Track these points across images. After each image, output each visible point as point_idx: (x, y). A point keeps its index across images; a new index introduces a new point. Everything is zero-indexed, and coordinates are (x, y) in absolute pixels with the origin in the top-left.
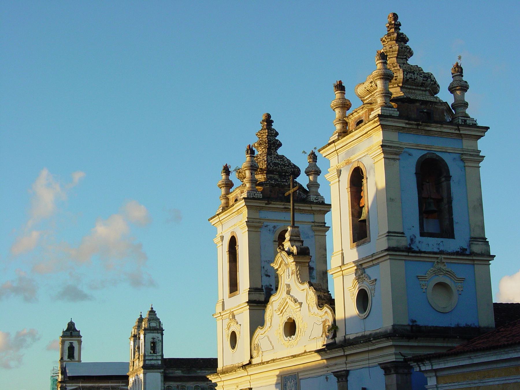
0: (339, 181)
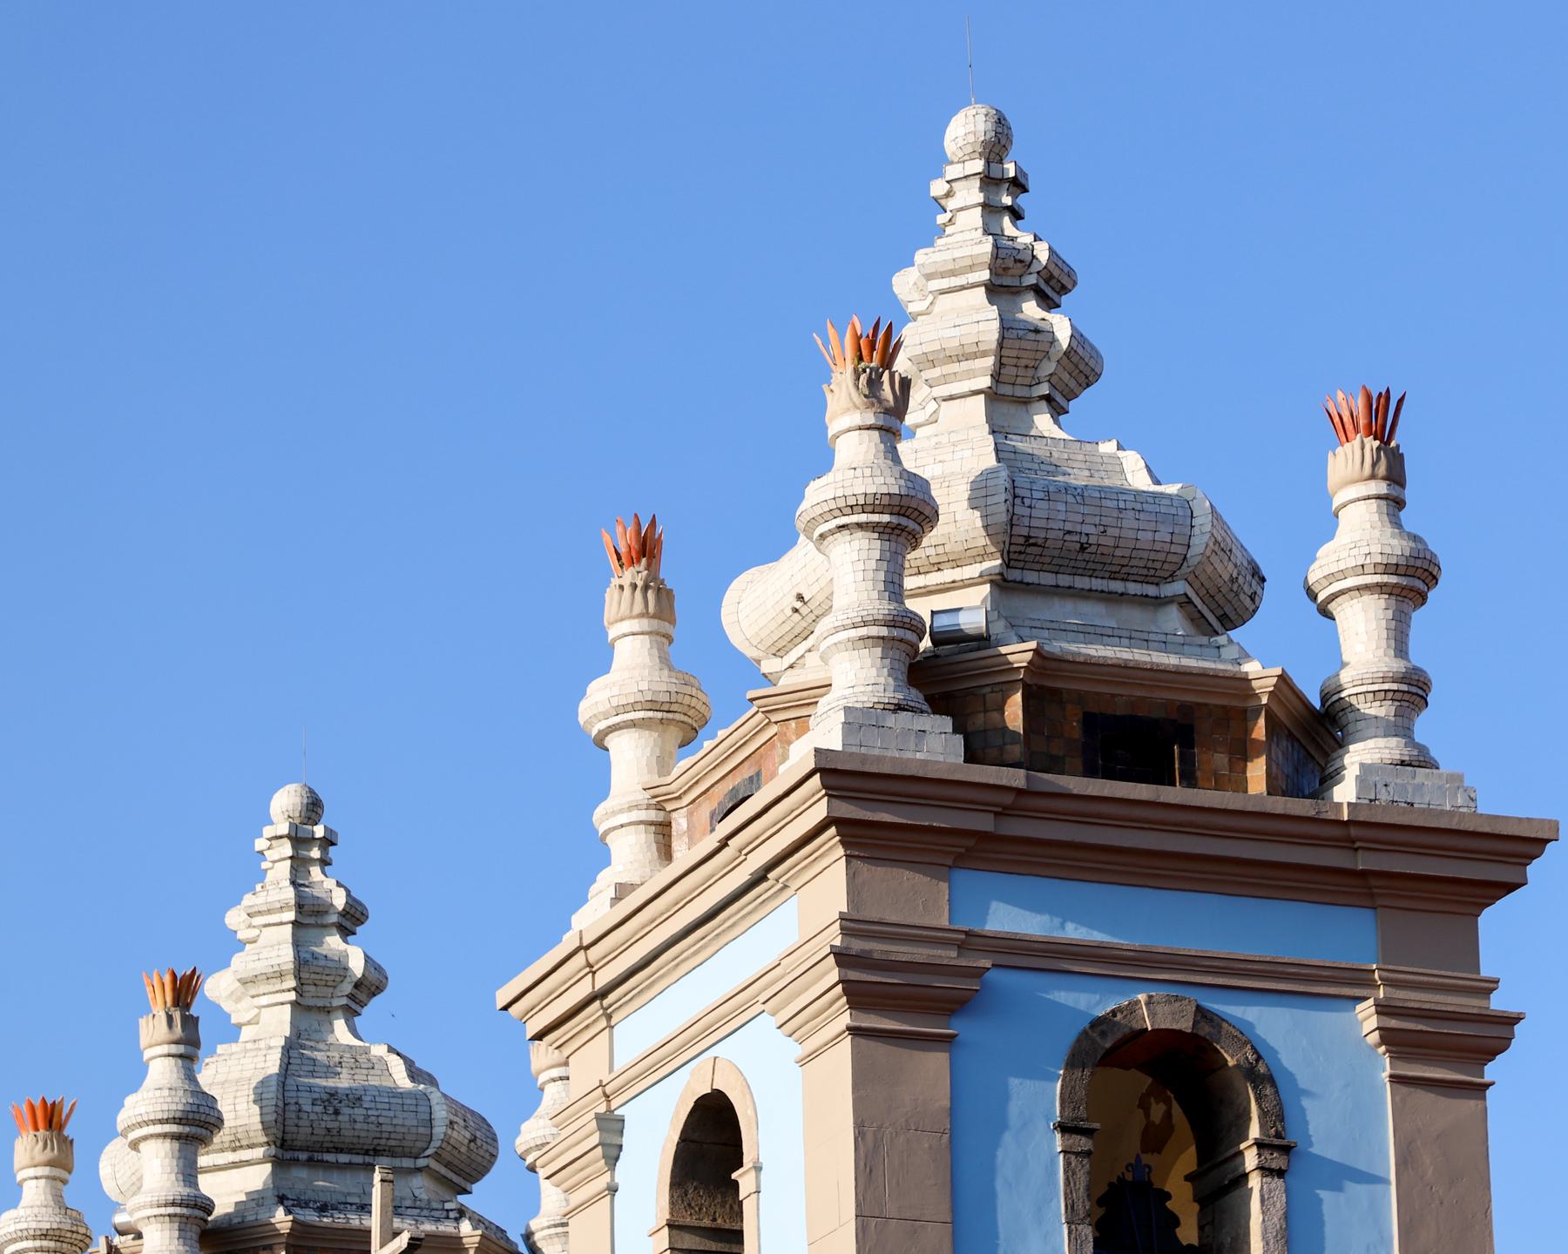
0: (613, 1190)
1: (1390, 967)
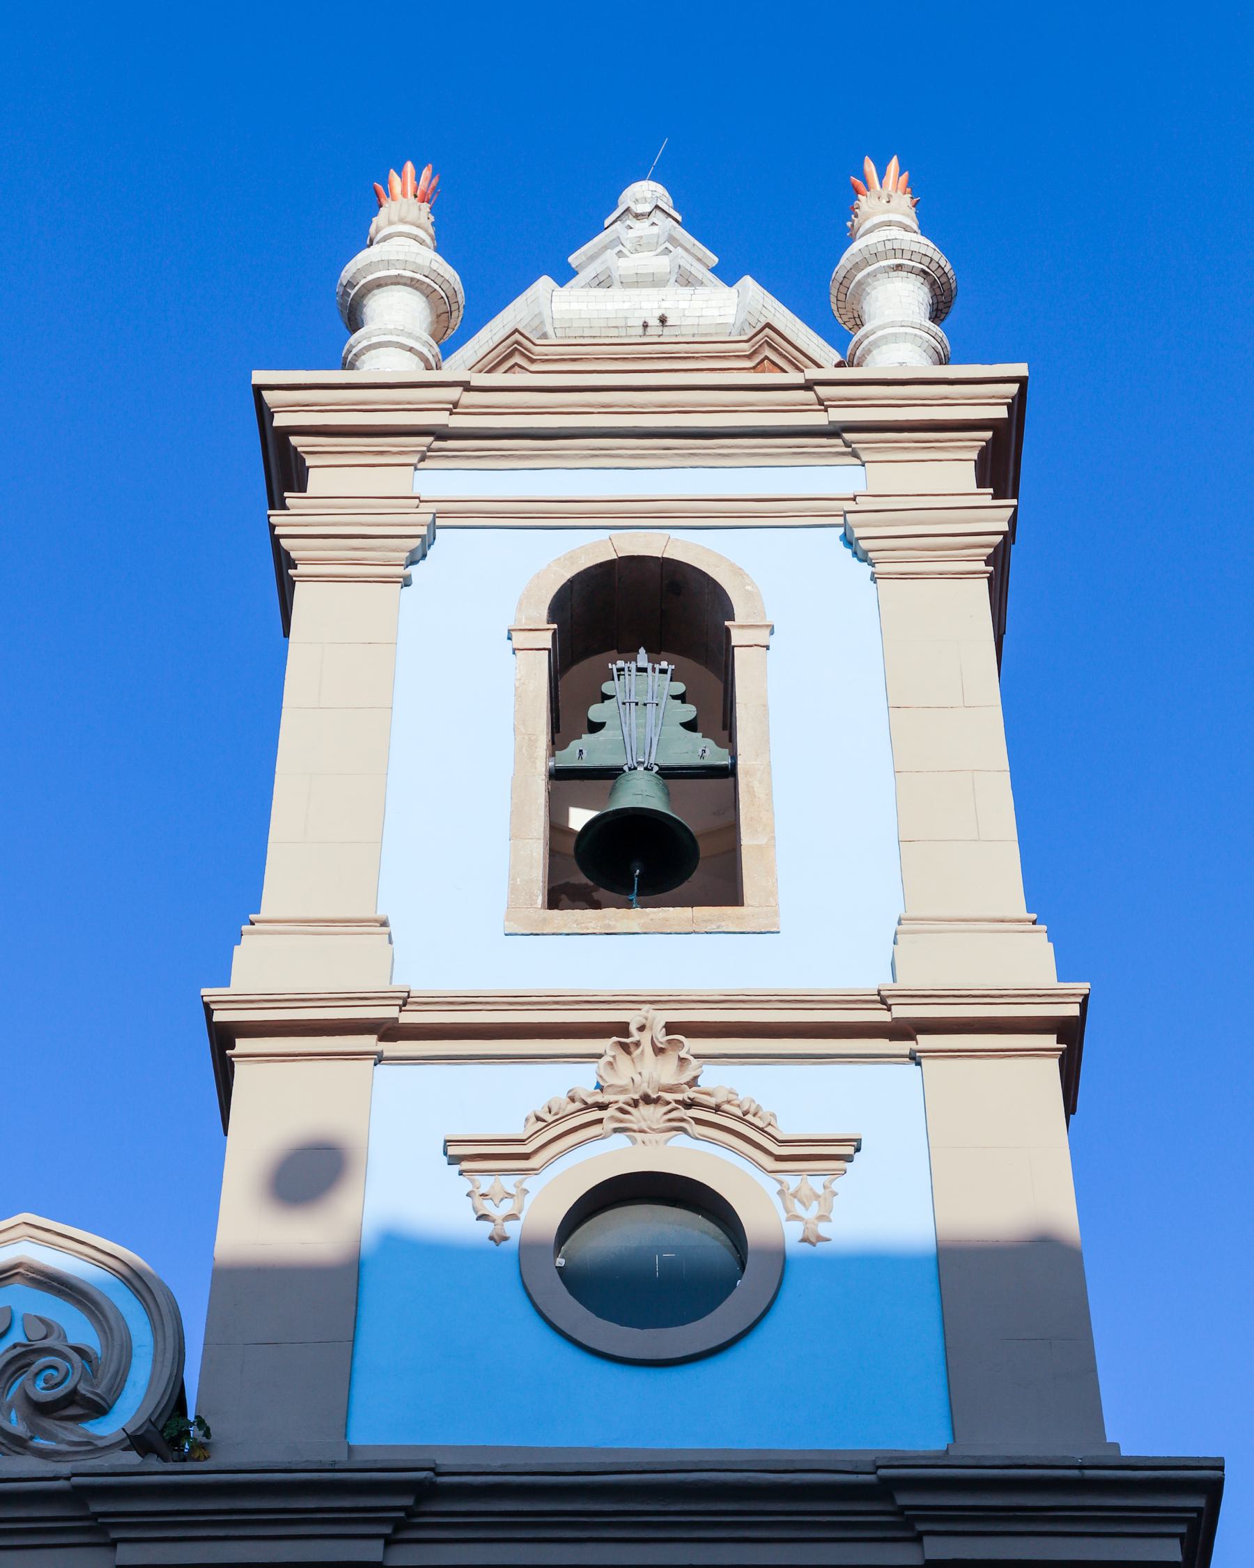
0: (407, 582)
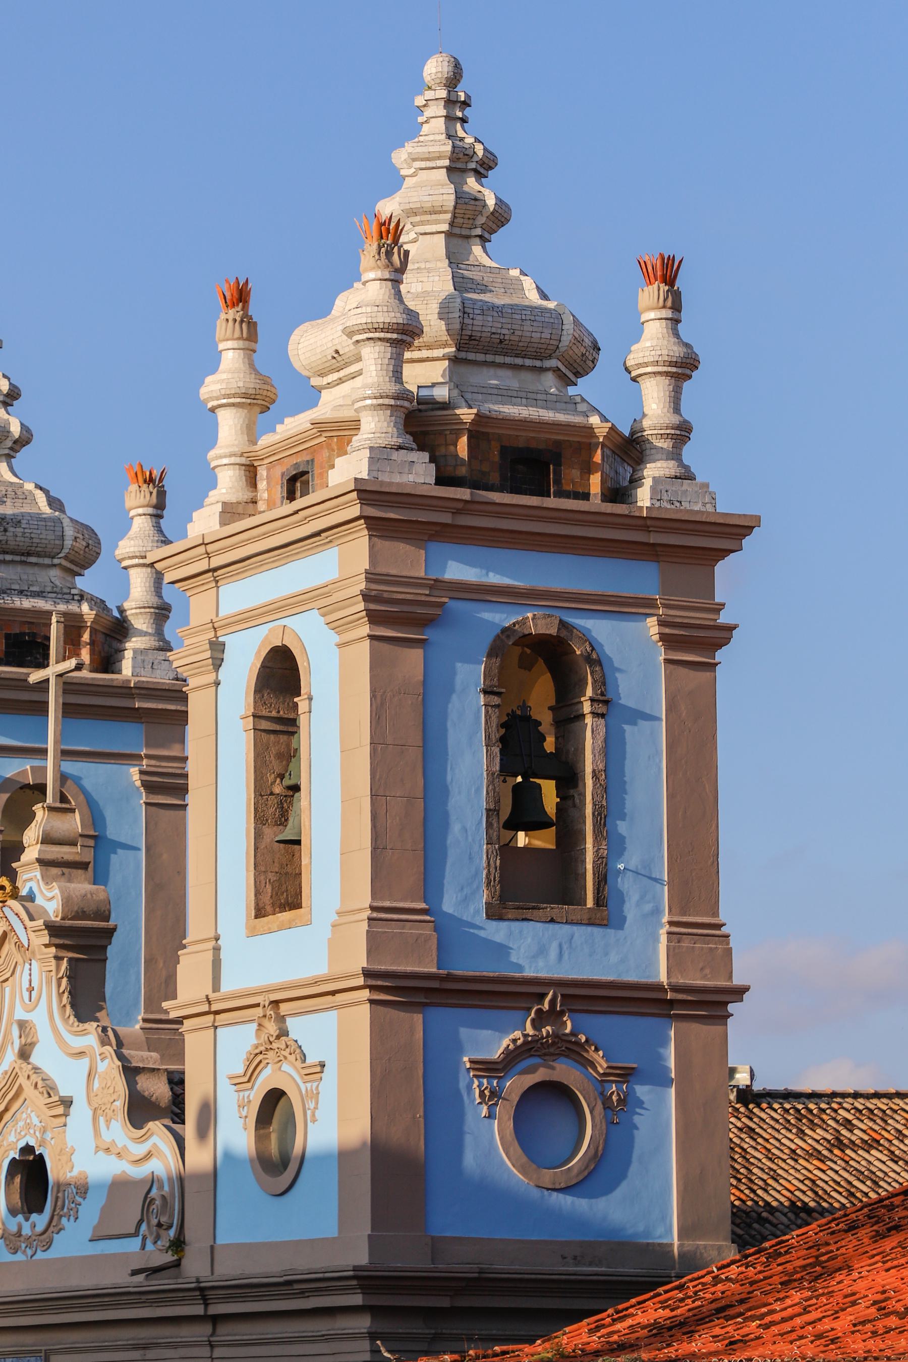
0: (217, 684)
1: (666, 597)
